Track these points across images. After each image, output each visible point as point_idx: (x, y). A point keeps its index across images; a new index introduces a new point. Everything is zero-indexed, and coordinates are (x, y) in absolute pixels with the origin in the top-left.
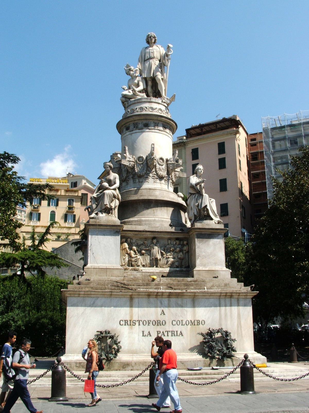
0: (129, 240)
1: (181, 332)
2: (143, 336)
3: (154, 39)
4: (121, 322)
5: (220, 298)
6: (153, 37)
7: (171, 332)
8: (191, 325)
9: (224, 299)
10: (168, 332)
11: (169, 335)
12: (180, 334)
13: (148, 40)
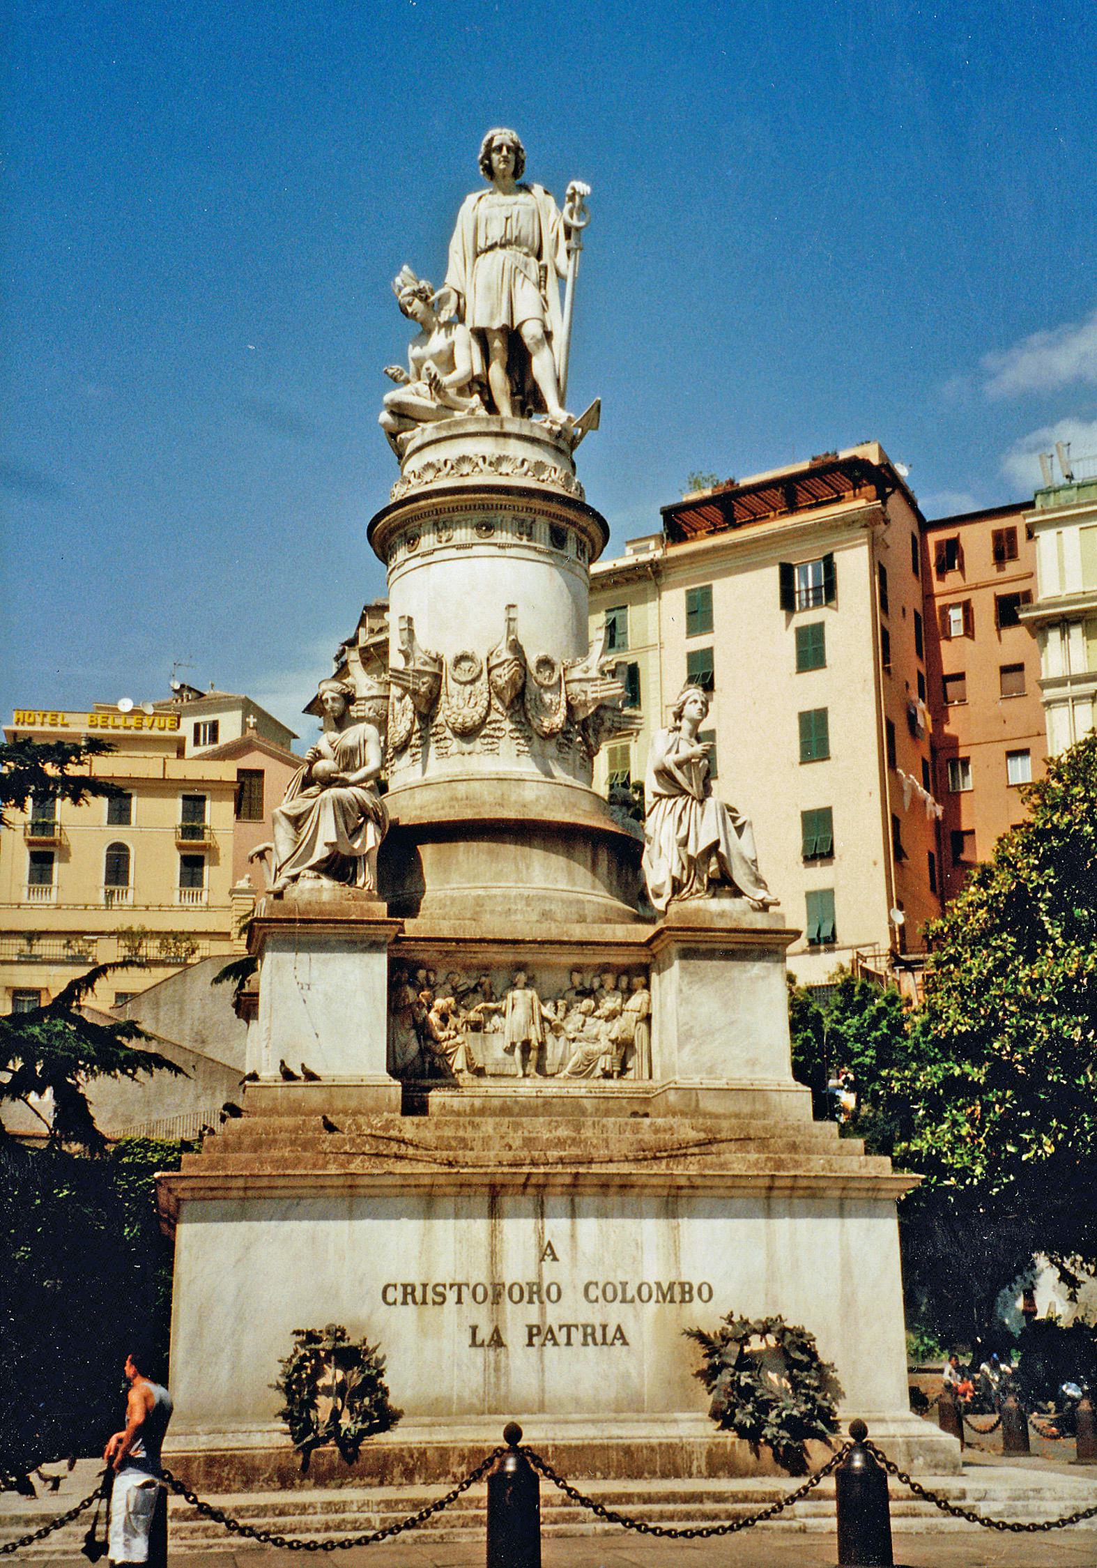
1: (619, 1329)
2: (473, 1344)
4: (391, 1290)
5: (768, 1198)
7: (581, 1329)
8: (657, 1301)
10: (569, 1327)
11: (572, 1341)
12: (615, 1337)
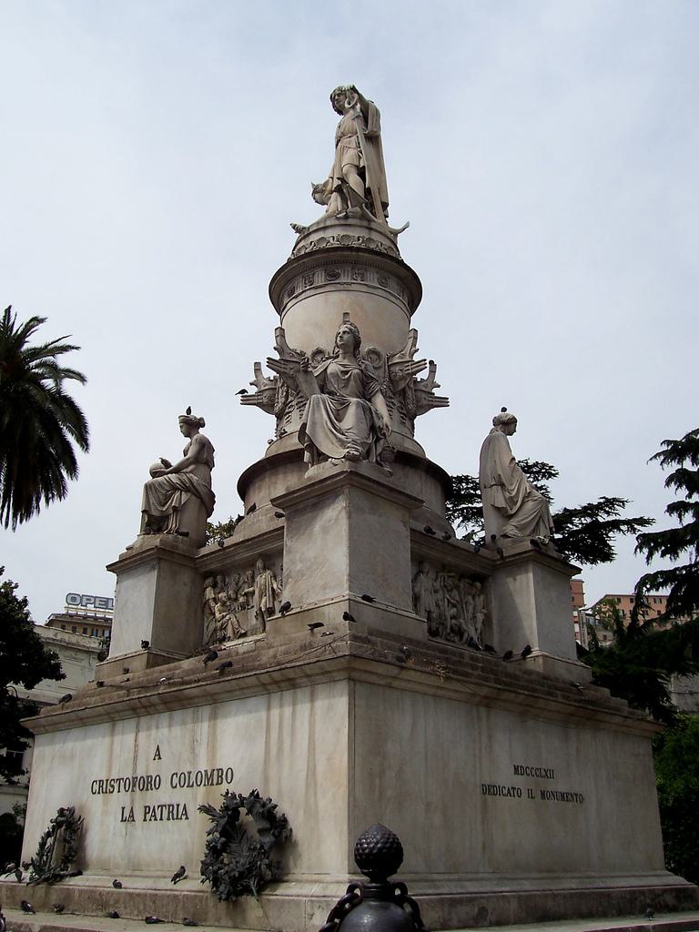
0: (219, 578)
2: (122, 821)
8: (205, 785)
9: (310, 688)
10: (162, 806)
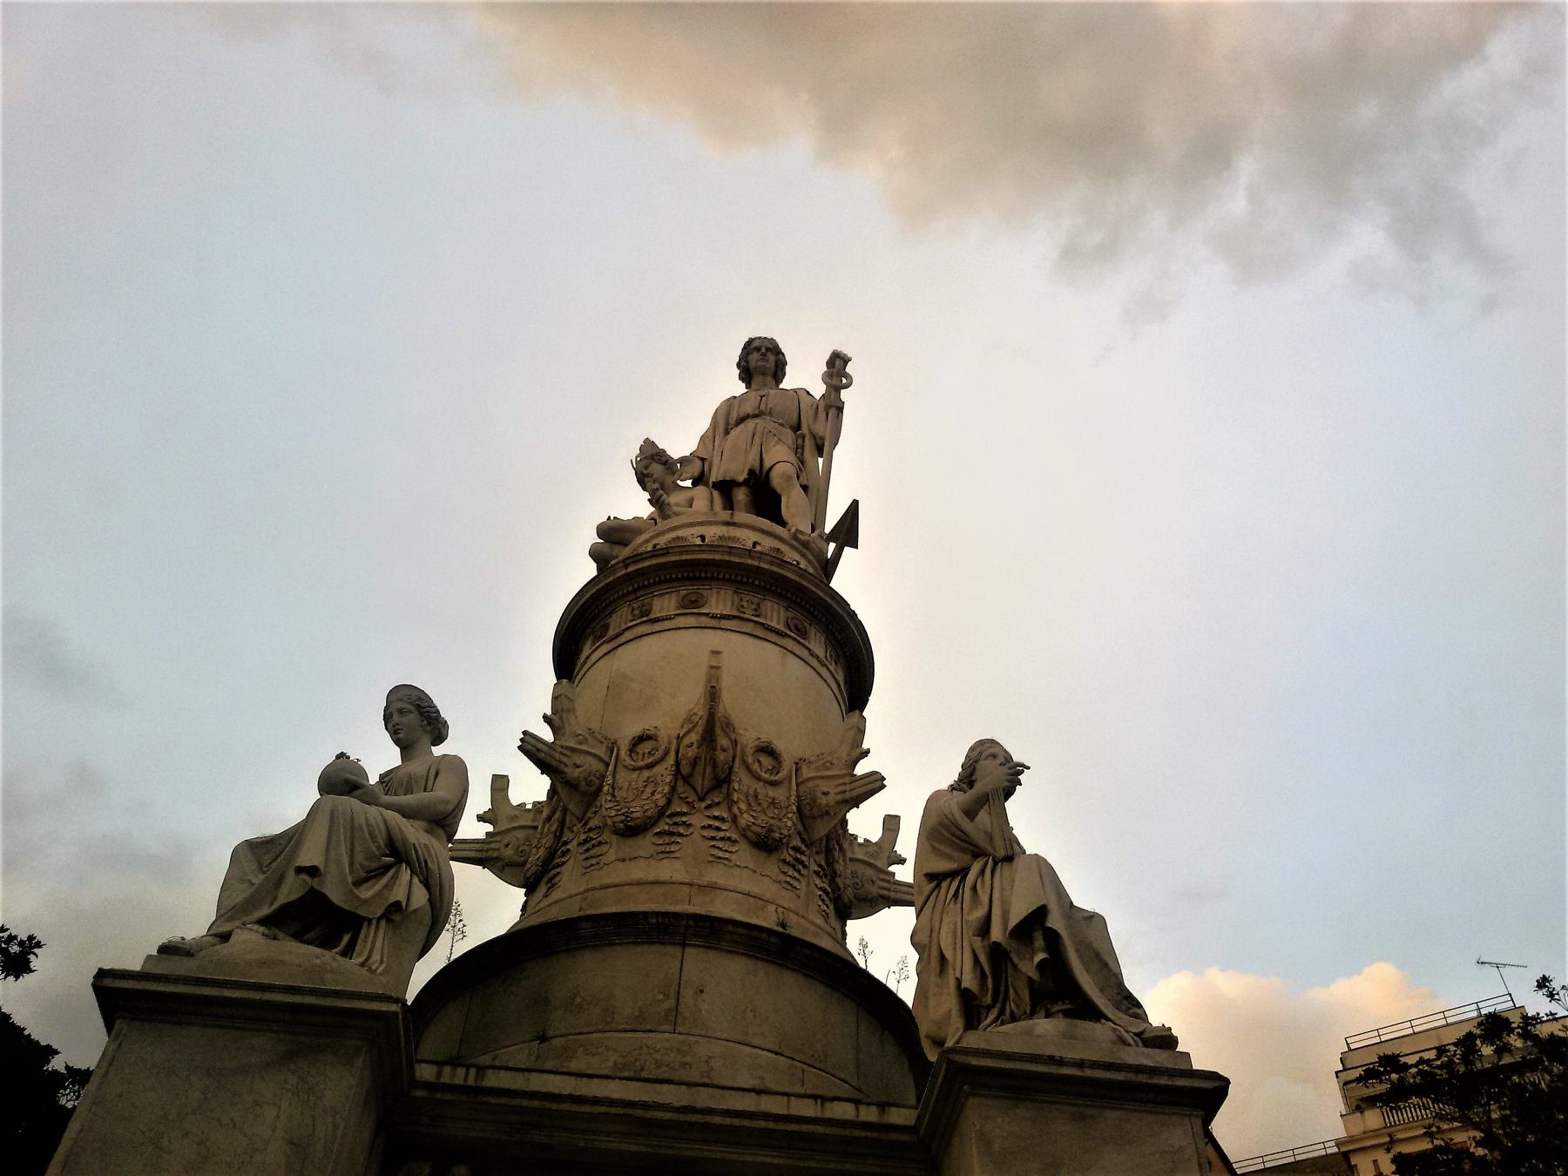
3: (771, 357)
6: (768, 349)
13: (747, 362)
